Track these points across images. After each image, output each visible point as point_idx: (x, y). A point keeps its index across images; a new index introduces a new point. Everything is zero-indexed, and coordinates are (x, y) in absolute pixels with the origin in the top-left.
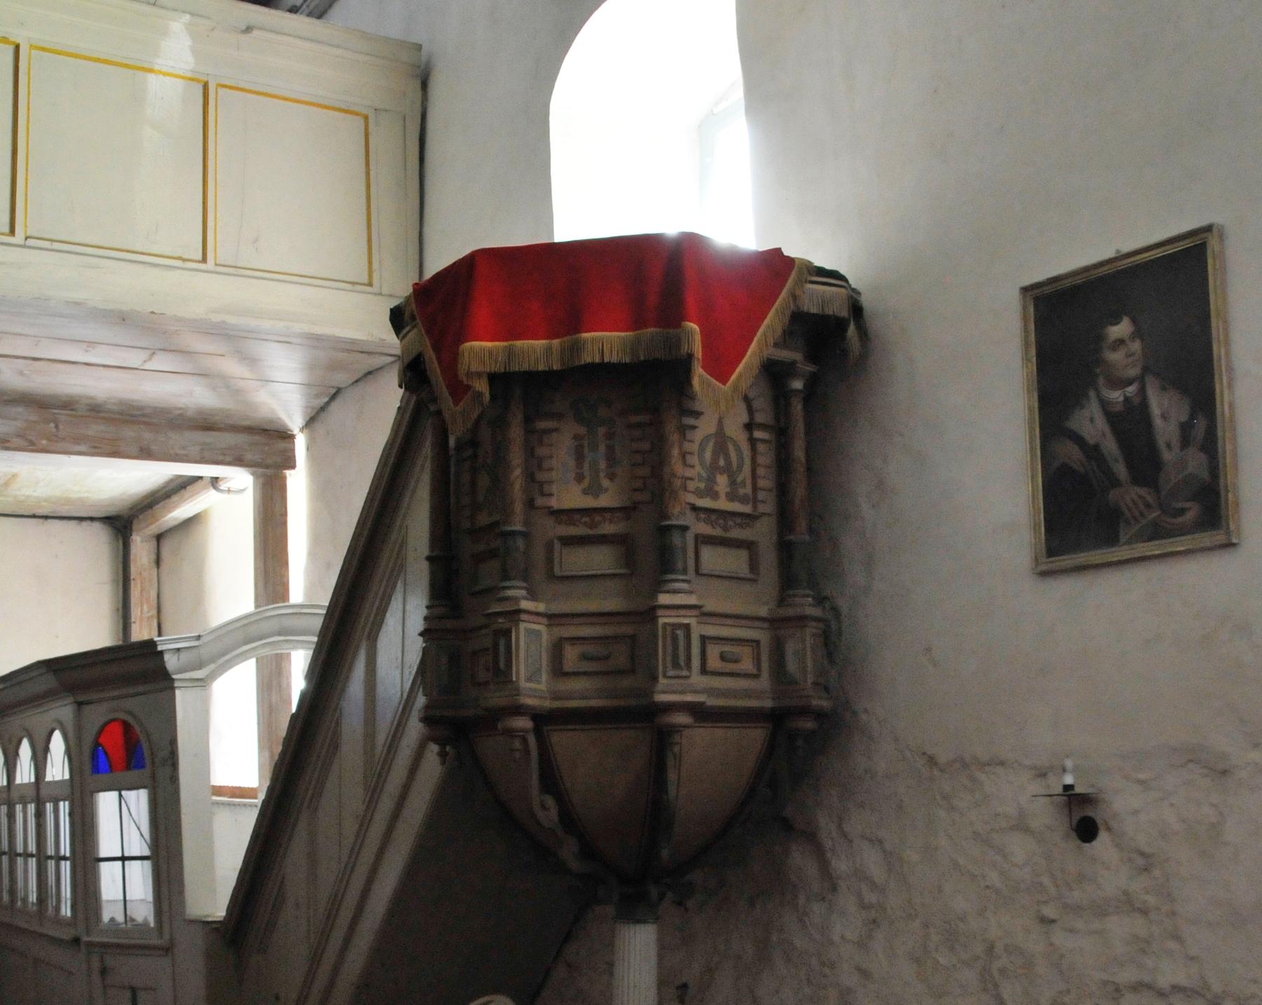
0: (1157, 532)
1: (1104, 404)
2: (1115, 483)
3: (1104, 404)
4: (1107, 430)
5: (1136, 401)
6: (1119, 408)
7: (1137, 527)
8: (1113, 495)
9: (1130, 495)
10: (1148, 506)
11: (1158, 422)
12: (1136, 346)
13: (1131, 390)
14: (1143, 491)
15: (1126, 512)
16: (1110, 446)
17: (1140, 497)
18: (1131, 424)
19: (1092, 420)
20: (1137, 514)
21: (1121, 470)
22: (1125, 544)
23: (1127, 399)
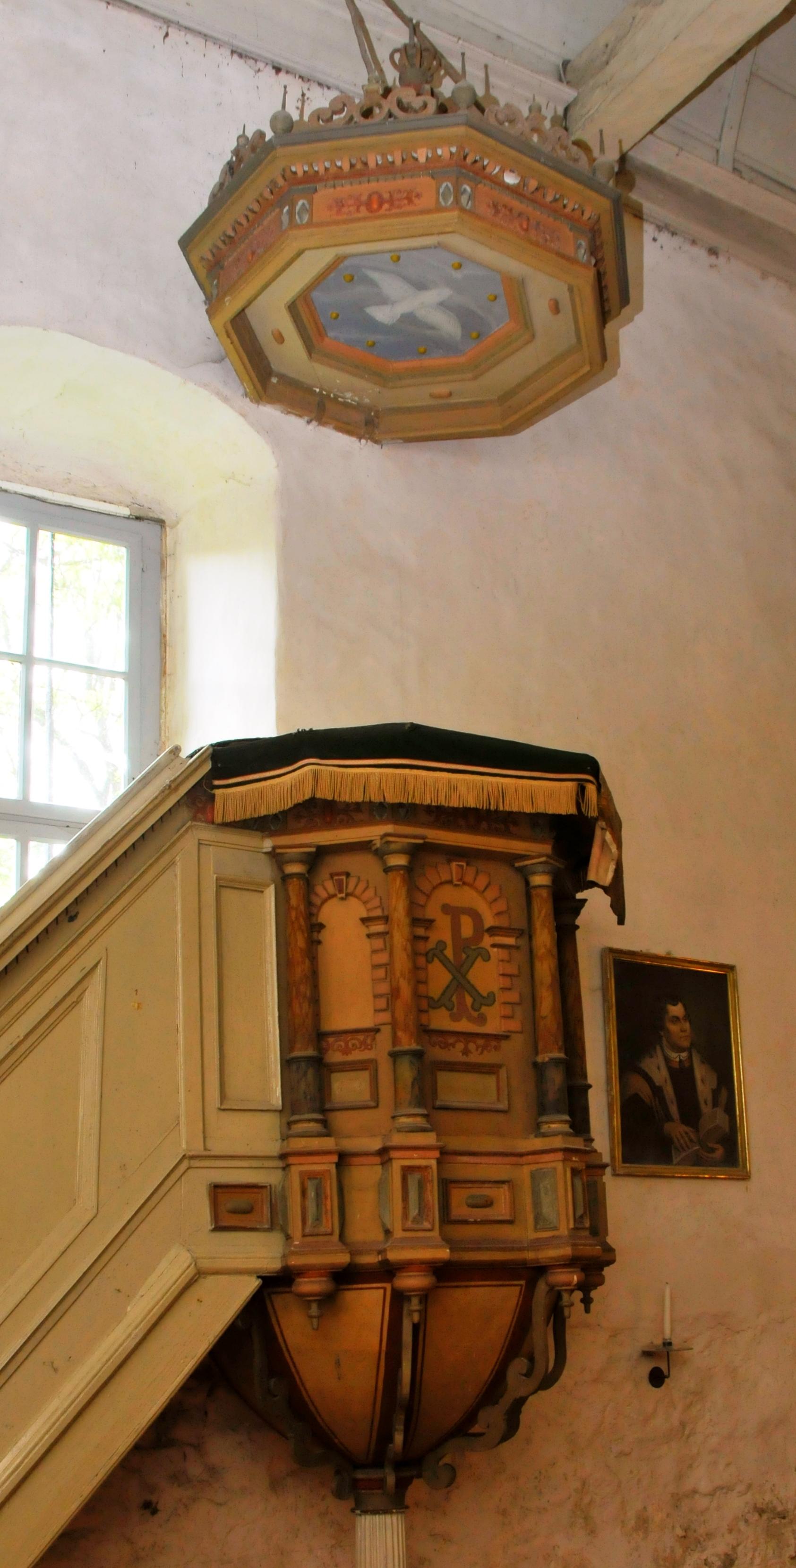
0: (698, 1161)
1: (667, 1060)
2: (669, 1118)
3: (667, 1060)
4: (668, 1077)
5: (687, 1065)
6: (677, 1066)
7: (684, 1154)
8: (668, 1127)
9: (677, 1129)
10: (691, 1140)
11: (699, 1083)
12: (687, 1026)
13: (684, 1055)
14: (687, 1129)
15: (676, 1140)
16: (669, 1091)
17: (686, 1133)
18: (682, 1077)
19: (659, 1068)
20: (684, 1145)
21: (674, 1109)
22: (678, 1164)
23: (681, 1061)
